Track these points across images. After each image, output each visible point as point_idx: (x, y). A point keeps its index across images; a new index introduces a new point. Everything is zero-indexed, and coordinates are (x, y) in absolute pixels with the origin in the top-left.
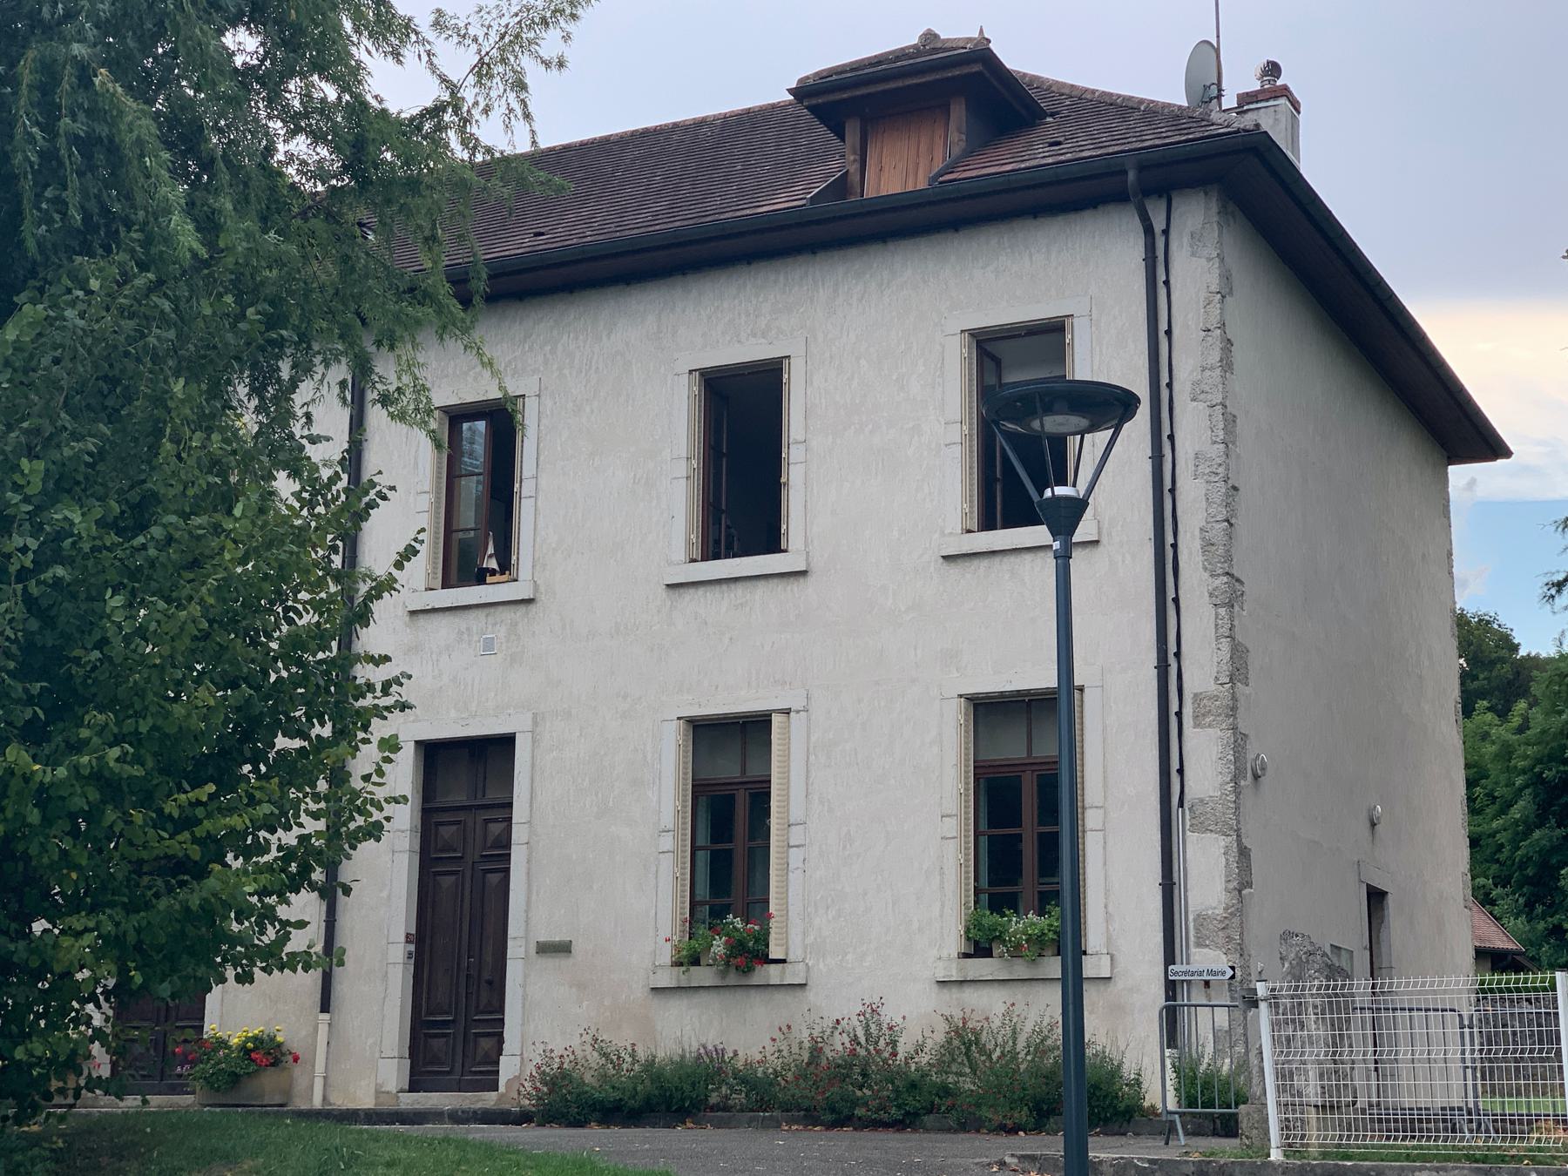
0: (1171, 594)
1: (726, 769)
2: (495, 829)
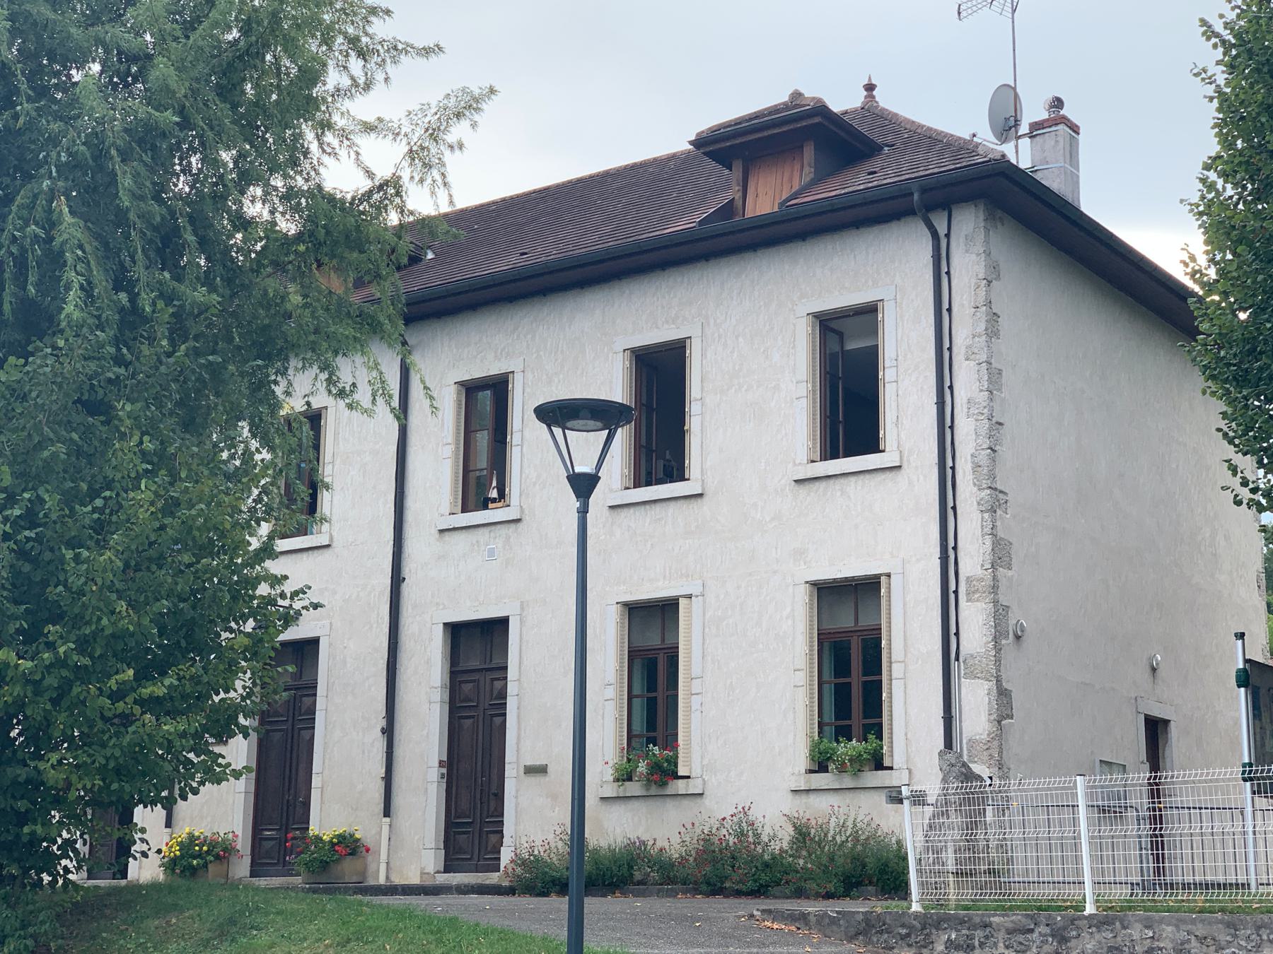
2: (498, 685)
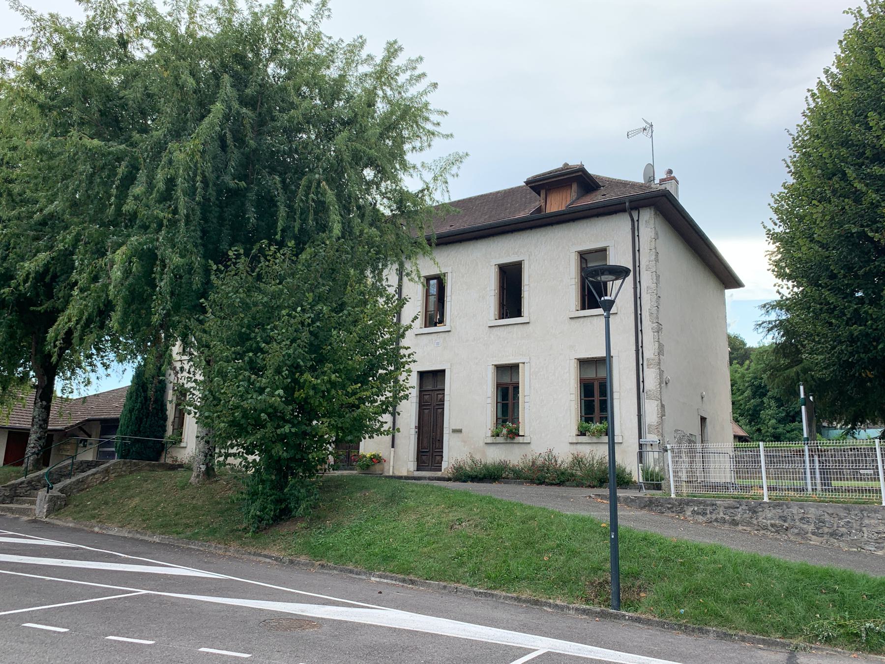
0: (640, 329)
1: (506, 380)
2: (440, 396)
